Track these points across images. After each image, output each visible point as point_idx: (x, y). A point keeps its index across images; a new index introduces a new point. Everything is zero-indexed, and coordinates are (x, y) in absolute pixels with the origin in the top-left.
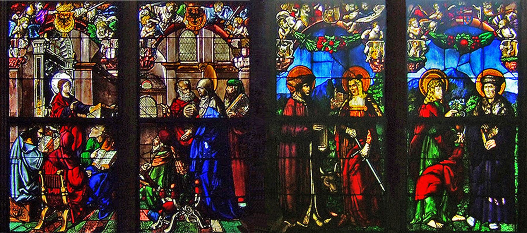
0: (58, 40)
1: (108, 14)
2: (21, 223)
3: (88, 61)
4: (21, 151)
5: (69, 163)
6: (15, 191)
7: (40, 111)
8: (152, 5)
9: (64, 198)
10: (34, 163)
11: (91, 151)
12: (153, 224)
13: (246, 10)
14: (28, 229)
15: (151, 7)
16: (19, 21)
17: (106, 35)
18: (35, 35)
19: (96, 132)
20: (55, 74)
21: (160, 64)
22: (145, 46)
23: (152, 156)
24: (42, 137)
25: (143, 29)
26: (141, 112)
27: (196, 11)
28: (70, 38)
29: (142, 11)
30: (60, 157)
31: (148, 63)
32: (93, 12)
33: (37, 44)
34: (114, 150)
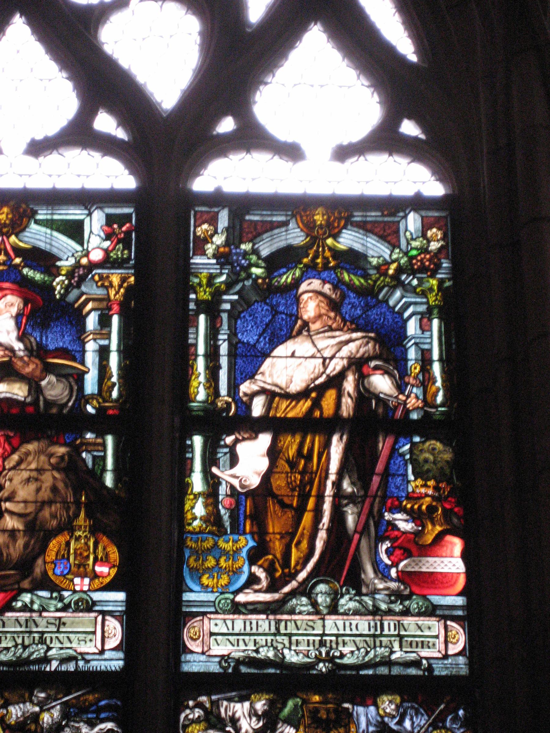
8: (214, 697)
13: (461, 712)
15: (212, 702)
27: (328, 713)
29: (188, 711)
32: (56, 713)
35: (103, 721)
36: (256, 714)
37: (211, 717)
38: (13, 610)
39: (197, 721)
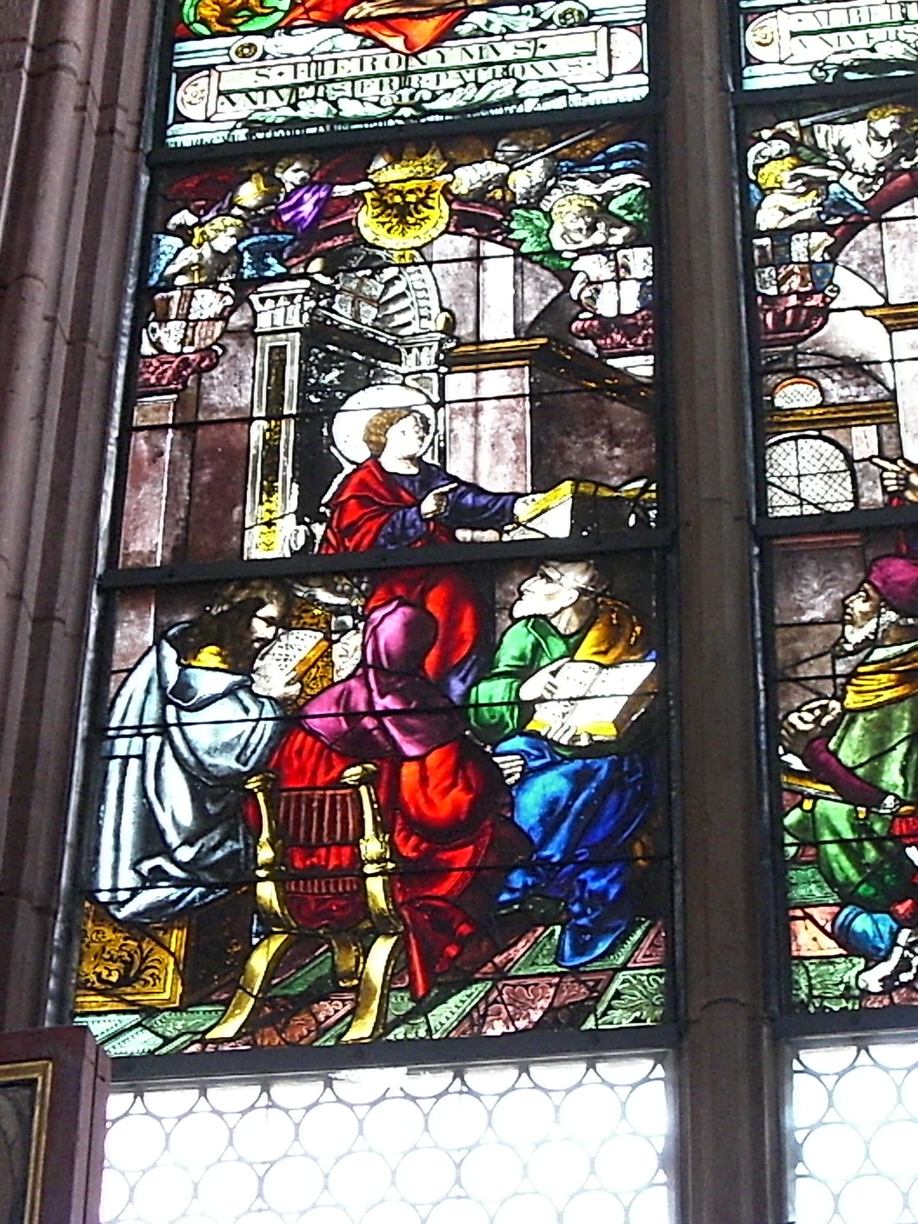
0: (372, 277)
1: (606, 171)
2: (134, 1018)
3: (513, 336)
4: (165, 701)
5: (406, 731)
6: (116, 869)
7: (273, 531)
8: (804, 122)
9: (375, 887)
10: (227, 747)
11: (524, 670)
12: (867, 968)
14: (167, 1041)
15: (801, 129)
16: (197, 231)
17: (598, 238)
18: (269, 267)
19: (553, 593)
20: (350, 394)
21: (858, 313)
22: (779, 257)
23: (842, 667)
24: (276, 637)
25: (770, 202)
26: (775, 497)
28: (430, 264)
29: (761, 145)
30: (362, 707)
31: (796, 317)
33: (276, 299)
34: (642, 660)
35: (615, 173)
36: (878, 138)
37: (800, 149)
38: (458, 37)
39: (780, 156)
